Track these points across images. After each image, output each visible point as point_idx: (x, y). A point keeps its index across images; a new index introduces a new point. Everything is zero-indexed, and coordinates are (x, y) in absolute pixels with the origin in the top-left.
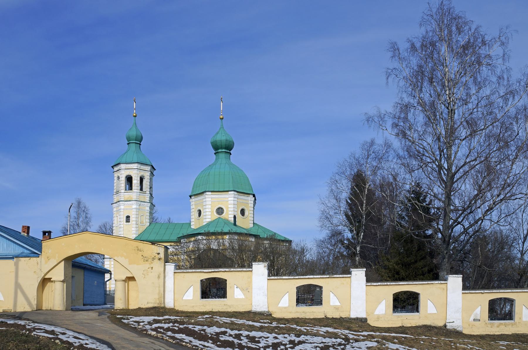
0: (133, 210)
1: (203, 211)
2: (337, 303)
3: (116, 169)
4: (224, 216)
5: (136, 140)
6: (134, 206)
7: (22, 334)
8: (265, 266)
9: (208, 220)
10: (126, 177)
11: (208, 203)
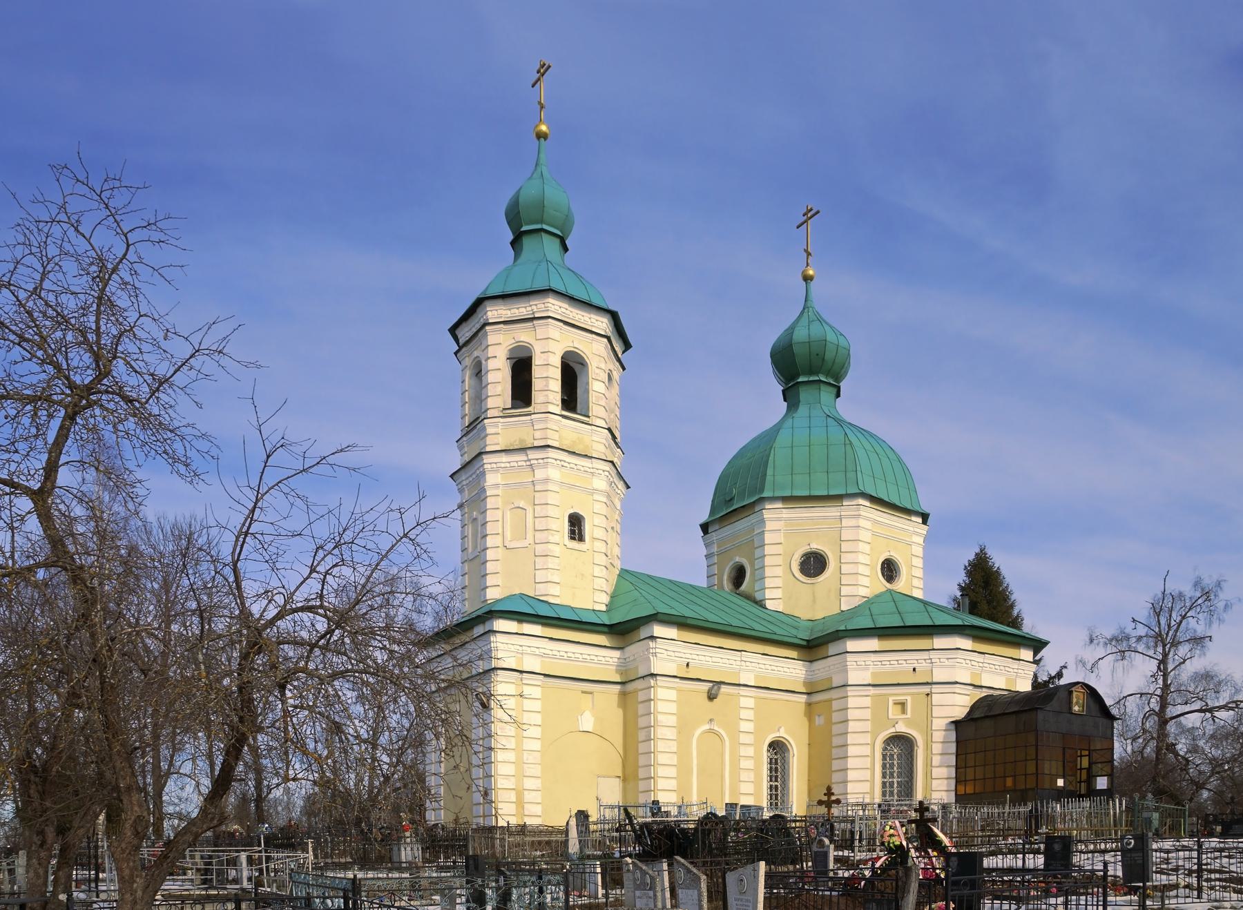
0: (596, 497)
4: (900, 585)
11: (865, 535)
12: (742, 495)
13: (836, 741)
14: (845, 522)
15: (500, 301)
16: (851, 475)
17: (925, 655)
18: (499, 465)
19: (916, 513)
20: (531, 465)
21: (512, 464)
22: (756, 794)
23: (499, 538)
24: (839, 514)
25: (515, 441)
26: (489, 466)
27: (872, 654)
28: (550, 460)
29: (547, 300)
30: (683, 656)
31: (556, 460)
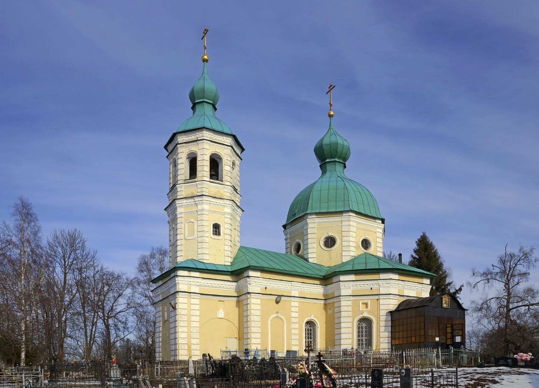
0: (226, 216)
4: (371, 251)
11: (353, 229)
12: (299, 213)
13: (337, 321)
14: (344, 223)
15: (183, 134)
16: (347, 202)
17: (376, 282)
18: (182, 204)
19: (379, 219)
20: (196, 204)
21: (188, 203)
22: (300, 345)
23: (183, 235)
24: (341, 220)
25: (190, 193)
26: (178, 205)
27: (351, 282)
28: (204, 201)
29: (202, 132)
30: (263, 284)
31: (207, 201)
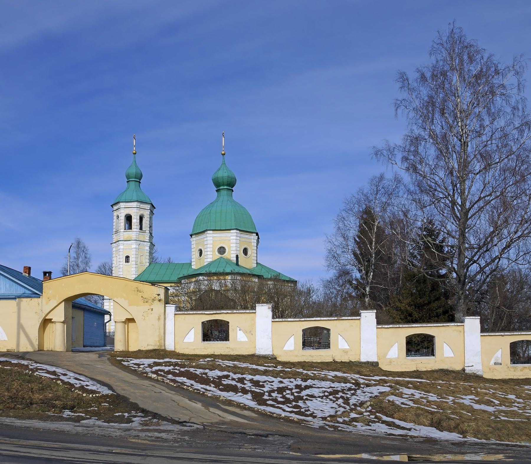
1: (204, 250)
2: (347, 347)
3: (115, 208)
4: (226, 255)
5: (135, 178)
6: (134, 246)
7: (26, 373)
8: (269, 308)
9: (210, 260)
10: (126, 216)
11: (209, 242)
